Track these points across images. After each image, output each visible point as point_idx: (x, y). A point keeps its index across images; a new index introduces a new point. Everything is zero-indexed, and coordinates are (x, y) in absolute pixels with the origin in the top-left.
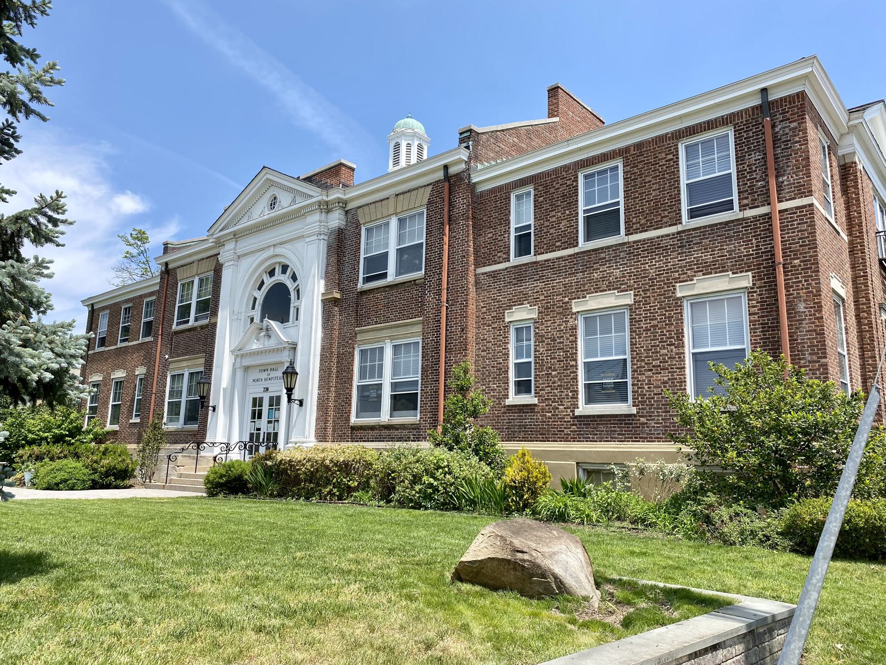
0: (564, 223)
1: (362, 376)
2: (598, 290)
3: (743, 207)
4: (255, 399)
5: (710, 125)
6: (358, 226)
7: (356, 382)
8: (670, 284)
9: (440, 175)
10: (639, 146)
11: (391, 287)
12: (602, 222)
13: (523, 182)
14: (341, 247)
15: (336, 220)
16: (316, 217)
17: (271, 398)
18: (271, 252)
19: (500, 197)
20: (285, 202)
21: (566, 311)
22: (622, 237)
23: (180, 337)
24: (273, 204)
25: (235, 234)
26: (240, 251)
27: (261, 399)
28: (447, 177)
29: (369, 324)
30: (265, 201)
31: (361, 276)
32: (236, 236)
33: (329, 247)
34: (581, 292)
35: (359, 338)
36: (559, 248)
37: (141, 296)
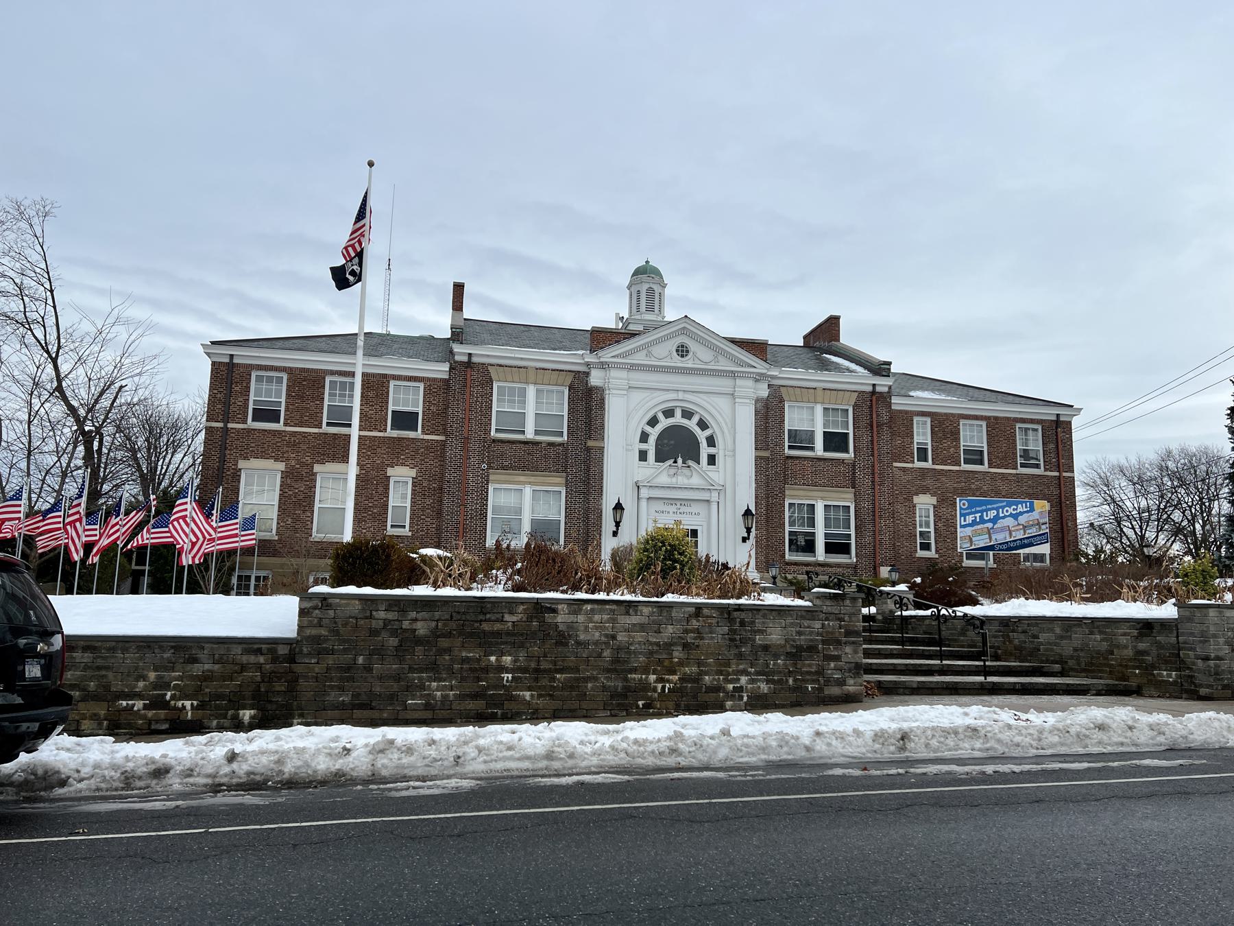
1: (792, 524)
3: (1046, 470)
5: (1032, 421)
6: (782, 401)
7: (787, 529)
9: (870, 389)
10: (996, 418)
11: (819, 459)
12: (975, 456)
13: (923, 414)
14: (769, 415)
15: (764, 392)
16: (750, 383)
18: (681, 396)
19: (907, 418)
20: (700, 355)
22: (984, 468)
23: (499, 447)
25: (632, 365)
26: (633, 383)
28: (873, 392)
30: (672, 345)
31: (787, 444)
32: (633, 367)
35: (787, 492)
36: (950, 464)
37: (385, 376)
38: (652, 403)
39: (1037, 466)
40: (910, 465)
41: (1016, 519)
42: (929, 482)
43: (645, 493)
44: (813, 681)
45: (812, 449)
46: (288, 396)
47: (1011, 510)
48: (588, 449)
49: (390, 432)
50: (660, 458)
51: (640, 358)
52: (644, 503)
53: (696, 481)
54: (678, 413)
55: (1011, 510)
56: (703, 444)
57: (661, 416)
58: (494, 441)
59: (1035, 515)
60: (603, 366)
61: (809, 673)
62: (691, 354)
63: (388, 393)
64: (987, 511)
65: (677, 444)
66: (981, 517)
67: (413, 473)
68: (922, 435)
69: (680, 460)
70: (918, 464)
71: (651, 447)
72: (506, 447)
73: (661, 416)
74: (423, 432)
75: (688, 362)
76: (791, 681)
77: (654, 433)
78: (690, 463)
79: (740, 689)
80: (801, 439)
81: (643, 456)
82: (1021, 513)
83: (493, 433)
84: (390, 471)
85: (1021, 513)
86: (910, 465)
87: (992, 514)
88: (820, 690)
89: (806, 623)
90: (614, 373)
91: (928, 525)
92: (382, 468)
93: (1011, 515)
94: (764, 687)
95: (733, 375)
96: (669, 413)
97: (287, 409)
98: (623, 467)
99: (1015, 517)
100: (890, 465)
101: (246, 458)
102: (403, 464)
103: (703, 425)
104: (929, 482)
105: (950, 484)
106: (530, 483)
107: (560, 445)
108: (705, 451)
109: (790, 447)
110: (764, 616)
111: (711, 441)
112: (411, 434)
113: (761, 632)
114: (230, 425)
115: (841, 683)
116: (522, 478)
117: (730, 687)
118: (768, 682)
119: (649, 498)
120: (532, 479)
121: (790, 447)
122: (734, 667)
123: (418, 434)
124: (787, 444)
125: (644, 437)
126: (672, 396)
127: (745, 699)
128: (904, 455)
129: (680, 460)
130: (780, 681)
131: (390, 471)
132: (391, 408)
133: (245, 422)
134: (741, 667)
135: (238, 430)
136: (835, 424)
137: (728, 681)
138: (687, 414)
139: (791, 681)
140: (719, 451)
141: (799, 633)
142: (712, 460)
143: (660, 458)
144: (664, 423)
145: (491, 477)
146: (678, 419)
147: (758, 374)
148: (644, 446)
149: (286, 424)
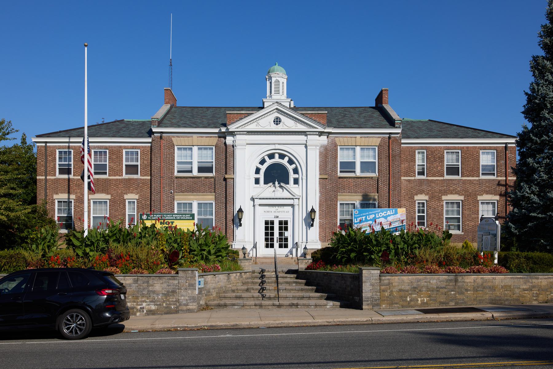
0: (439, 167)
2: (451, 193)
4: (266, 223)
7: (339, 217)
8: (476, 195)
12: (453, 170)
14: (328, 156)
17: (280, 223)
18: (278, 147)
21: (440, 200)
24: (277, 121)
27: (272, 222)
29: (344, 192)
31: (339, 170)
33: (321, 154)
34: (446, 193)
35: (339, 197)
36: (437, 176)
37: (120, 147)
38: (261, 151)
39: (494, 174)
40: (413, 178)
41: (386, 219)
42: (424, 187)
43: (257, 202)
44: (174, 304)
45: (354, 172)
46: (74, 160)
47: (383, 214)
48: (225, 179)
49: (125, 176)
50: (266, 183)
51: (252, 127)
52: (257, 207)
53: (286, 194)
54: (277, 156)
55: (383, 214)
56: (291, 172)
57: (267, 158)
58: (177, 178)
59: (398, 216)
60: (232, 134)
61: (172, 301)
62: (281, 124)
63: (122, 155)
64: (369, 215)
65: (276, 174)
66: (366, 218)
67: (137, 197)
68: (419, 160)
69: (277, 183)
70: (418, 177)
71: (261, 176)
72: (183, 180)
73: (267, 158)
74: (141, 175)
75: (279, 128)
76: (164, 305)
77: (263, 168)
78: (282, 184)
79: (143, 308)
80: (349, 166)
81: (257, 181)
82: (389, 215)
83: (176, 174)
84: (126, 197)
85: (389, 215)
86: (413, 178)
87: (372, 216)
88: (177, 307)
89: (171, 281)
90: (238, 137)
91: (423, 212)
92: (122, 194)
93: (383, 217)
94: (153, 307)
95: (304, 133)
96: (271, 156)
97: (74, 168)
98: (246, 187)
99: (386, 217)
100: (399, 179)
101: (57, 194)
102: (132, 193)
103: (291, 162)
104: (424, 187)
105: (437, 188)
106: (196, 199)
107: (212, 177)
108: (292, 176)
109: (341, 172)
110: (153, 279)
111: (296, 171)
112: (135, 176)
113: (152, 285)
114: (48, 177)
115: (187, 305)
116: (192, 197)
117: (139, 307)
118: (155, 305)
119: (260, 205)
120: (197, 197)
121: (341, 172)
122: (140, 299)
123: (138, 176)
124: (339, 170)
125: (258, 171)
126: (273, 147)
127: (145, 312)
128: (410, 172)
129: (277, 183)
130: (160, 305)
131: (126, 197)
132: (124, 163)
133: (55, 175)
134: (143, 299)
135: (52, 180)
136: (369, 157)
137: (137, 305)
138: (282, 156)
139: (164, 305)
140: (301, 176)
141: (168, 286)
142: (296, 181)
143: (266, 183)
144: (269, 162)
145: (176, 197)
146: (277, 159)
147: (319, 132)
148: (257, 176)
149: (74, 175)
